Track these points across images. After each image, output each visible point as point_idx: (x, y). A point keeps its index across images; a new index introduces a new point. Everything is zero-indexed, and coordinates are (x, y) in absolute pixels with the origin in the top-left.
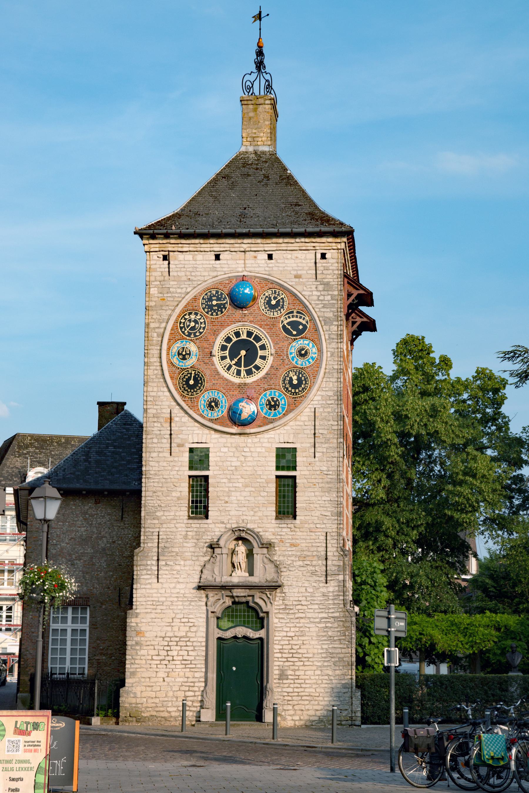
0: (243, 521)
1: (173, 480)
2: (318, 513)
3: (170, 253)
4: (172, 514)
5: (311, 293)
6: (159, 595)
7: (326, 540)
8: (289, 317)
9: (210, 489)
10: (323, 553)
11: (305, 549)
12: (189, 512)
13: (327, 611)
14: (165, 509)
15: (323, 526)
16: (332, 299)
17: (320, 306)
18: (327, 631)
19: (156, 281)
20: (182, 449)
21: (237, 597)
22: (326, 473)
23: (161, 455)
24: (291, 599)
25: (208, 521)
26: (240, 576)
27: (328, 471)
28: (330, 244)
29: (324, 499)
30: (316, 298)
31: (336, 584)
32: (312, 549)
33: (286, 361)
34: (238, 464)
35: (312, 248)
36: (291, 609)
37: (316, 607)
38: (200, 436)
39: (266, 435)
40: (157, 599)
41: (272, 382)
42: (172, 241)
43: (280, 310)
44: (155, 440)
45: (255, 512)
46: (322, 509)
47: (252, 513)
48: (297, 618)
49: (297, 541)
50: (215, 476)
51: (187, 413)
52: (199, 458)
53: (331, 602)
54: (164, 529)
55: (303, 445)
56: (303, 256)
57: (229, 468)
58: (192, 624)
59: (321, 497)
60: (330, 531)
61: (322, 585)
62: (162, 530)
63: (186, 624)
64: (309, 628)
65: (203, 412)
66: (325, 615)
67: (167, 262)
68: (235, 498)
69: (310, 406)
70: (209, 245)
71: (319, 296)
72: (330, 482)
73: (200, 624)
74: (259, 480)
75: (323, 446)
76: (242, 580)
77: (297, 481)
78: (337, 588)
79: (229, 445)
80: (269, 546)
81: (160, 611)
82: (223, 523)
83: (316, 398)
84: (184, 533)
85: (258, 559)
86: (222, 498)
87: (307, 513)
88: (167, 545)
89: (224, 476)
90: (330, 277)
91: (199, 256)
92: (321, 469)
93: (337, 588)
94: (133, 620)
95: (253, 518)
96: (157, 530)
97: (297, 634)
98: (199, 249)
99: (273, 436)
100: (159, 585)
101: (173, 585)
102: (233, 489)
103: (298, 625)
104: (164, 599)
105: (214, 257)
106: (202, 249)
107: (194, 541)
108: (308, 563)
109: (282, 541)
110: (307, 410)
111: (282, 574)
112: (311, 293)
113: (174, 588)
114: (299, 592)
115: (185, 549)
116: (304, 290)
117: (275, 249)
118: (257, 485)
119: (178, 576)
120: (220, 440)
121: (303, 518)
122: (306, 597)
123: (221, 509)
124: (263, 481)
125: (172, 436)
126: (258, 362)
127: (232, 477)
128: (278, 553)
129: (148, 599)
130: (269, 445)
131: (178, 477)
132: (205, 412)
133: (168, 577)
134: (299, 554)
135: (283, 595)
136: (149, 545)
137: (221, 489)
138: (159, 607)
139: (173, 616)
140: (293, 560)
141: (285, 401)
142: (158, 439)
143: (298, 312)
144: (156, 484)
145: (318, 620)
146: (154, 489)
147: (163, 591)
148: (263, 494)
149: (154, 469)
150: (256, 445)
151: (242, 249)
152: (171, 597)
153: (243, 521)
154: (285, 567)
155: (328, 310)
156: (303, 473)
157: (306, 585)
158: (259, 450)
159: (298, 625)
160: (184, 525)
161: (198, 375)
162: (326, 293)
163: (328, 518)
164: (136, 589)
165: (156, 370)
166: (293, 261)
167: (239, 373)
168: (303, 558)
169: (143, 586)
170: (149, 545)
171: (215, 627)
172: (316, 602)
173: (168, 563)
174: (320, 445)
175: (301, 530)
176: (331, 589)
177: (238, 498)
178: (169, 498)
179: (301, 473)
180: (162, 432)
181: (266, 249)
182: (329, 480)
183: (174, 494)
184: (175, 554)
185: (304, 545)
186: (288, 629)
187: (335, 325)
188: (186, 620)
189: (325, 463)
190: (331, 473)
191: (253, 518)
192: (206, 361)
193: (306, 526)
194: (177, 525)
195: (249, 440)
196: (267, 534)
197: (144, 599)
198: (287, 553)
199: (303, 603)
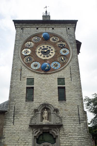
1: (21, 88)
6: (13, 130)
9: (34, 91)
11: (71, 111)
12: (26, 99)
13: (81, 135)
14: (18, 98)
17: (69, 40)
18: (82, 143)
20: (24, 78)
21: (45, 130)
22: (76, 85)
23: (17, 80)
25: (33, 102)
26: (45, 122)
27: (77, 85)
30: (67, 38)
31: (83, 124)
32: (73, 111)
33: (59, 53)
34: (44, 83)
36: (66, 134)
37: (77, 133)
38: (31, 74)
39: (54, 74)
40: (12, 131)
41: (55, 59)
42: (24, 24)
45: (51, 99)
46: (75, 97)
47: (50, 99)
48: (69, 138)
49: (67, 109)
51: (26, 67)
52: (31, 81)
53: (82, 131)
54: (17, 105)
55: (67, 77)
57: (41, 84)
58: (26, 142)
59: (75, 93)
60: (79, 105)
61: (78, 125)
63: (24, 142)
64: (74, 142)
65: (32, 67)
66: (80, 136)
67: (22, 30)
72: (78, 89)
73: (30, 141)
75: (74, 77)
77: (66, 88)
78: (84, 126)
79: (41, 77)
80: (56, 110)
81: (13, 136)
82: (39, 103)
83: (70, 63)
85: (53, 116)
88: (18, 111)
89: (39, 87)
90: (71, 33)
91: (32, 29)
94: (2, 140)
95: (50, 101)
96: (14, 105)
97: (70, 144)
98: (32, 27)
100: (14, 126)
101: (19, 126)
102: (43, 91)
103: (70, 141)
104: (15, 131)
105: (36, 29)
107: (28, 109)
108: (72, 116)
109: (61, 109)
111: (62, 121)
114: (69, 128)
115: (24, 112)
118: (51, 90)
120: (38, 76)
123: (38, 98)
125: (22, 75)
126: (50, 54)
127: (42, 87)
129: (9, 131)
131: (23, 87)
132: (33, 68)
133: (18, 122)
135: (63, 129)
136: (11, 111)
138: (13, 135)
139: (19, 138)
141: (60, 64)
142: (16, 75)
144: (14, 90)
145: (77, 139)
146: (14, 91)
147: (15, 128)
148: (53, 92)
149: (14, 85)
151: (45, 27)
153: (46, 102)
154: (63, 118)
156: (67, 86)
157: (72, 125)
158: (51, 78)
159: (70, 141)
160: (24, 104)
161: (31, 58)
162: (70, 37)
163: (78, 100)
167: (44, 57)
169: (7, 127)
170: (11, 111)
171: (36, 142)
173: (18, 117)
174: (73, 77)
175: (68, 105)
176: (82, 126)
179: (67, 86)
180: (18, 74)
182: (77, 88)
183: (21, 93)
184: (20, 114)
185: (70, 110)
186: (66, 143)
188: (24, 140)
190: (77, 85)
191: (50, 101)
192: (34, 53)
194: (21, 104)
196: (55, 106)
197: (7, 132)
198: (64, 113)
199: (71, 132)
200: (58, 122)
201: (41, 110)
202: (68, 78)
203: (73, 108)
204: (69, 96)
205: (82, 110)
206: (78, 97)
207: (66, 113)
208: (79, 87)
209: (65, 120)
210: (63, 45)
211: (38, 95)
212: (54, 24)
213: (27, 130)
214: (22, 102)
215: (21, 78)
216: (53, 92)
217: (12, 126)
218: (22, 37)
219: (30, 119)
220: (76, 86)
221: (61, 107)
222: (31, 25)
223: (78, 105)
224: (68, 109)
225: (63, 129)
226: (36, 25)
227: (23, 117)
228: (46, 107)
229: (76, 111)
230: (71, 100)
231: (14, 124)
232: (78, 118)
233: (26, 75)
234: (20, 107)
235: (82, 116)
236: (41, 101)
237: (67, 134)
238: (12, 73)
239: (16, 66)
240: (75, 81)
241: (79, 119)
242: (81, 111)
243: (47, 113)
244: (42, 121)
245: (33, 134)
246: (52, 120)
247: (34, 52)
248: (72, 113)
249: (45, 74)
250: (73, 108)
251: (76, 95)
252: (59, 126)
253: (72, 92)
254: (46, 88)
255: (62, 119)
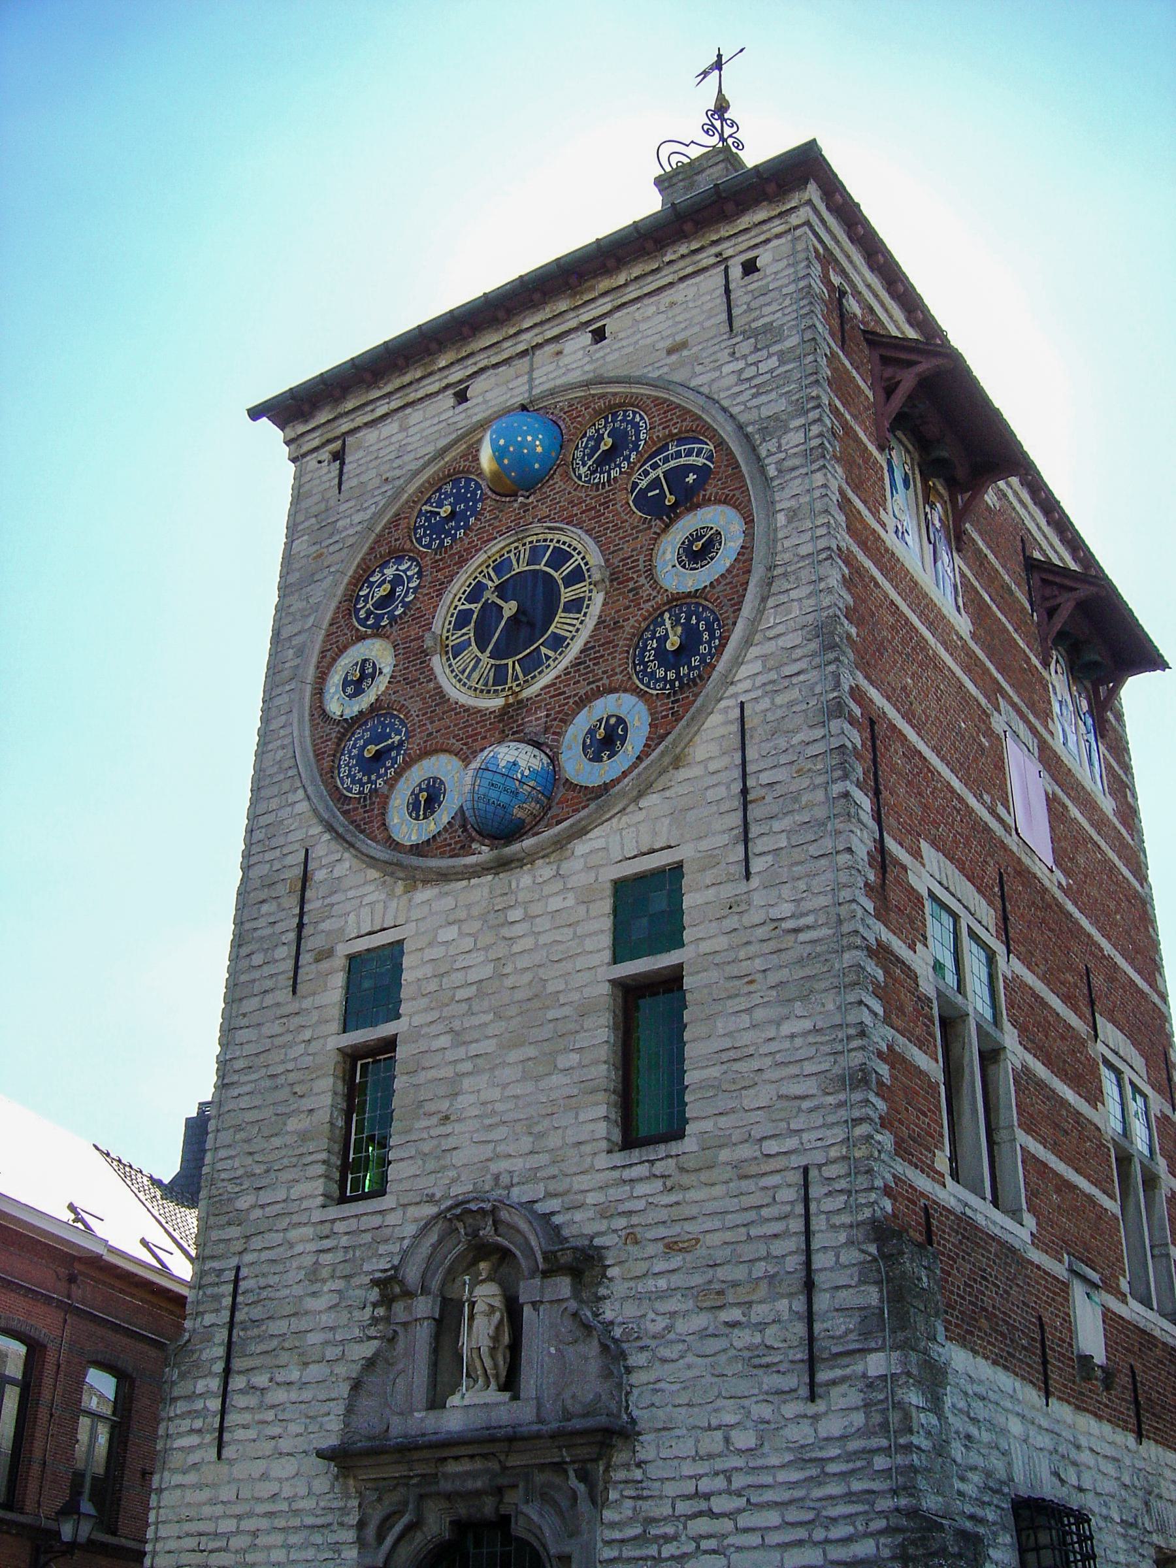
0: (497, 1178)
2: (763, 1095)
3: (350, 440)
4: (281, 1195)
5: (717, 374)
7: (806, 1200)
8: (655, 466)
10: (794, 1263)
11: (720, 1255)
13: (819, 1534)
15: (791, 1143)
16: (782, 362)
19: (307, 519)
20: (325, 965)
22: (790, 924)
23: (269, 1000)
24: (670, 1489)
26: (471, 1406)
27: (803, 915)
28: (765, 227)
29: (787, 1029)
30: (733, 379)
32: (748, 1251)
34: (488, 970)
35: (713, 260)
36: (668, 1539)
37: (772, 1518)
42: (349, 405)
43: (627, 458)
44: (257, 959)
45: (541, 1135)
47: (526, 1143)
49: (688, 1227)
50: (416, 1033)
55: (704, 845)
56: (691, 292)
57: (461, 994)
59: (779, 1024)
60: (819, 1157)
61: (791, 1409)
62: (248, 1258)
68: (472, 1098)
69: (723, 704)
70: (437, 377)
71: (741, 371)
74: (551, 1015)
76: (478, 1420)
78: (858, 1419)
79: (462, 914)
80: (583, 1265)
83: (743, 671)
84: (308, 1261)
86: (430, 1107)
87: (723, 1103)
88: (257, 1313)
91: (415, 416)
92: (775, 913)
93: (858, 1419)
96: (234, 1262)
98: (413, 396)
99: (601, 843)
100: (224, 1468)
101: (258, 1467)
102: (467, 1066)
104: (228, 1525)
105: (451, 401)
106: (420, 394)
107: (339, 1284)
108: (735, 1314)
109: (632, 1238)
110: (714, 719)
111: (635, 1378)
112: (717, 374)
113: (264, 1477)
114: (698, 1457)
116: (695, 375)
117: (609, 307)
119: (276, 1430)
120: (437, 906)
121: (708, 1125)
122: (728, 1474)
123: (426, 1147)
124: (567, 1011)
128: (620, 1289)
130: (586, 879)
131: (307, 1061)
134: (697, 1280)
135: (638, 1474)
136: (209, 1319)
137: (431, 1074)
140: (673, 1314)
143: (681, 441)
148: (563, 1061)
150: (547, 890)
151: (521, 347)
152: (250, 1515)
155: (773, 395)
156: (705, 947)
157: (730, 1419)
158: (555, 903)
163: (806, 1105)
164: (160, 1491)
165: (283, 747)
166: (662, 317)
168: (713, 1298)
170: (209, 1319)
172: (769, 1496)
175: (704, 1176)
176: (832, 1426)
177: (484, 1096)
178: (276, 1142)
179: (701, 950)
181: (585, 318)
183: (293, 1124)
184: (275, 1343)
185: (715, 1239)
187: (797, 429)
189: (786, 891)
190: (809, 920)
193: (724, 1155)
195: (523, 879)
196: (578, 1216)
198: (650, 1284)
199: (719, 1504)
200: (589, 1386)
201: (435, 1285)
202: (711, 860)
203: (751, 1215)
204: (715, 1072)
205: (846, 1219)
206: (809, 1068)
207: (676, 1280)
208: (825, 932)
209: (664, 1361)
210: (691, 478)
211: (424, 1123)
212: (604, 284)
213: (322, 1504)
214: (295, 1219)
215: (297, 967)
216: (563, 1061)
217: (211, 1472)
218: (331, 535)
219: (344, 1389)
220: (796, 931)
221: (635, 1220)
222: (407, 379)
223: (806, 1170)
224: (692, 1228)
225: (638, 1474)
226: (443, 364)
227: (295, 1375)
228: (479, 1235)
229: (778, 1247)
230: (733, 1111)
231: (226, 1453)
232: (800, 1329)
233: (342, 930)
234: (279, 1268)
235: (846, 1298)
236: (452, 1173)
237: (675, 1538)
238: (239, 941)
239: (269, 856)
240: (784, 874)
241: (811, 1338)
242: (842, 1238)
243: (497, 1302)
244: (436, 1403)
245: (361, 1542)
246: (529, 1382)
247: (414, 659)
248: (739, 1273)
249: (502, 865)
250: (751, 1215)
251: (787, 1044)
252: (598, 1441)
253: (745, 1020)
254: (498, 1027)
255: (631, 1361)
